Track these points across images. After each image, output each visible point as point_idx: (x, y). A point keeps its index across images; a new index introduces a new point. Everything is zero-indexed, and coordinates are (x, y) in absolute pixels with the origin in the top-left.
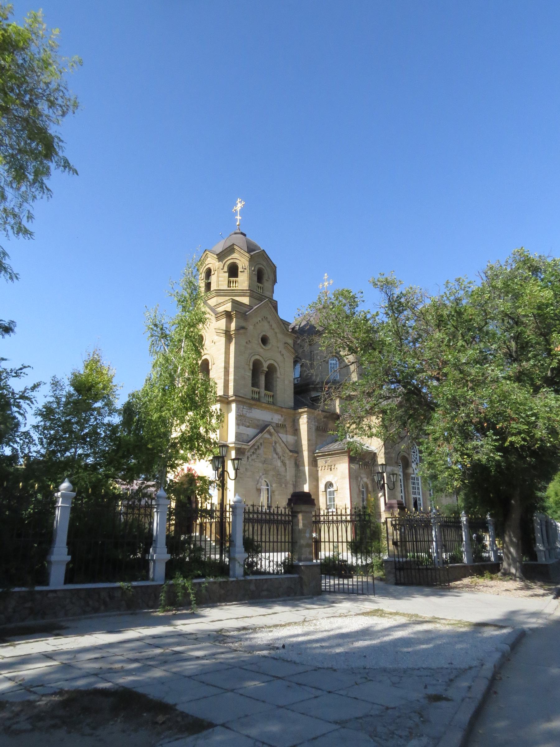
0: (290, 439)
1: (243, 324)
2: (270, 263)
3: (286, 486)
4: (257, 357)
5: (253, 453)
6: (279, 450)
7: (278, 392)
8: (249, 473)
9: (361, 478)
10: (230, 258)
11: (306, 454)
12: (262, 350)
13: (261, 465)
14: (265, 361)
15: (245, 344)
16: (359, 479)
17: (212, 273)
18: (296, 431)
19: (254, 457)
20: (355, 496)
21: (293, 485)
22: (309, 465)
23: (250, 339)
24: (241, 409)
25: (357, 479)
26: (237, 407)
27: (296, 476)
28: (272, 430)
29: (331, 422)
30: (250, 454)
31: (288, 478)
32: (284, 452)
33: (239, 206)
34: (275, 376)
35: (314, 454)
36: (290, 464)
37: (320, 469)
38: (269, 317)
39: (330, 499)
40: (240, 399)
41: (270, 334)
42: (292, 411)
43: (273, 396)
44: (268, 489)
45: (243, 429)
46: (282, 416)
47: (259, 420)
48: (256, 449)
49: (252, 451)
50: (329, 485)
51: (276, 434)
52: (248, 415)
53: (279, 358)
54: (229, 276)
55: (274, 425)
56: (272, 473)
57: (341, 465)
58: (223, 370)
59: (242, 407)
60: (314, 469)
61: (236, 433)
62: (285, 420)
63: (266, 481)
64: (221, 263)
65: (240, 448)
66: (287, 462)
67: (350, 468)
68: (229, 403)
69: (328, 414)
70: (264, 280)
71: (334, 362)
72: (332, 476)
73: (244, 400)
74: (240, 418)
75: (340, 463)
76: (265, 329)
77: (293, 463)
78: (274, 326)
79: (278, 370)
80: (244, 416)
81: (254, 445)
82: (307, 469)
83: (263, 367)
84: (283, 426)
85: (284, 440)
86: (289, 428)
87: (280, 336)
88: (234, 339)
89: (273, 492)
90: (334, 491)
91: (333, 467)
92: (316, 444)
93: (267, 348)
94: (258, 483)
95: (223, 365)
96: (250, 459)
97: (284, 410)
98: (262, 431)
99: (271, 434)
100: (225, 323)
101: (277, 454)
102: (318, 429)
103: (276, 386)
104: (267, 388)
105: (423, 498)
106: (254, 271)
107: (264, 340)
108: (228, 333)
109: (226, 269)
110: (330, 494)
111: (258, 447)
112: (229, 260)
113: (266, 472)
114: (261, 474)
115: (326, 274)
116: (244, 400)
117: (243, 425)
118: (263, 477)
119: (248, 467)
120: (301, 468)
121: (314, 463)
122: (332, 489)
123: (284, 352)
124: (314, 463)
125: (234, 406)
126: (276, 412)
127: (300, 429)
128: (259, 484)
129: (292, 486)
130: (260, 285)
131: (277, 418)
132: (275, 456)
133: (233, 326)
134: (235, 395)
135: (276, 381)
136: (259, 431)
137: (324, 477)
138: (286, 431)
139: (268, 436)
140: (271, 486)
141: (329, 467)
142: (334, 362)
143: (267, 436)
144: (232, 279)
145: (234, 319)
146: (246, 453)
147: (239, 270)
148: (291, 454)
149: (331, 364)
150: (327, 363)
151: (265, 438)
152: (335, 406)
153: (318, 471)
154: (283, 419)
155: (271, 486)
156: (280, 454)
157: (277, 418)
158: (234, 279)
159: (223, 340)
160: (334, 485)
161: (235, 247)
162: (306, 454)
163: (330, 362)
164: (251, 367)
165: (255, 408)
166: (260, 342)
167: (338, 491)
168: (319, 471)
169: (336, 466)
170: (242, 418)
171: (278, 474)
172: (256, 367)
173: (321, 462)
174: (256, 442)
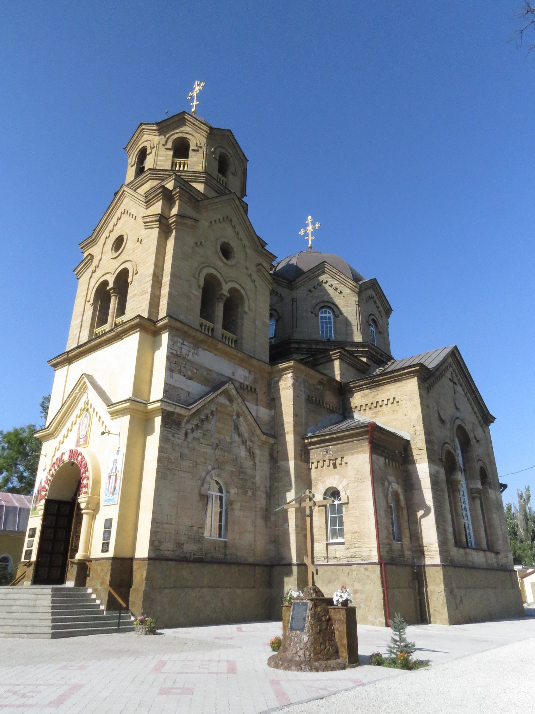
0: (264, 413)
1: (191, 213)
2: (239, 152)
3: (253, 494)
4: (215, 272)
5: (197, 426)
6: (243, 428)
7: (244, 335)
8: (186, 464)
9: (389, 483)
10: (177, 131)
11: (290, 438)
12: (221, 264)
13: (210, 451)
14: (226, 282)
15: (194, 245)
16: (386, 484)
17: (148, 152)
18: (273, 402)
19: (198, 434)
20: (382, 513)
21: (267, 493)
22: (295, 458)
23: (203, 242)
24: (179, 345)
25: (383, 484)
26: (170, 339)
27: (270, 479)
28: (234, 392)
29: (328, 392)
30: (190, 426)
31: (258, 479)
32: (252, 433)
33: (197, 89)
34: (240, 310)
35: (304, 439)
36: (262, 456)
37: (314, 465)
38: (234, 219)
39: (333, 520)
40: (178, 325)
41: (234, 244)
42: (267, 368)
43: (236, 341)
44: (221, 498)
45: (180, 381)
46: (250, 372)
47: (211, 371)
48: (202, 421)
49: (195, 422)
50: (334, 493)
51: (240, 400)
52: (190, 357)
53: (249, 285)
54: (175, 156)
55: (237, 385)
56: (229, 468)
57: (356, 456)
58: (151, 277)
59: (180, 341)
60: (304, 465)
61: (166, 384)
62: (255, 381)
63: (218, 483)
64: (162, 137)
65: (173, 413)
66: (257, 452)
67: (372, 463)
68: (156, 333)
69: (325, 378)
70: (229, 173)
71: (327, 315)
72: (337, 477)
73: (186, 329)
74: (175, 360)
75: (353, 454)
76: (228, 235)
77: (267, 454)
78: (242, 235)
79: (246, 301)
80: (184, 358)
81: (198, 412)
82: (292, 464)
83: (221, 289)
84: (252, 390)
85: (254, 414)
86: (261, 396)
87: (250, 252)
88: (174, 231)
89: (230, 503)
90: (341, 505)
91: (338, 461)
92: (307, 425)
93: (229, 263)
94: (202, 485)
95: (152, 270)
96: (190, 437)
97: (255, 362)
98: (215, 389)
99: (231, 400)
100: (160, 207)
101: (240, 435)
102: (309, 400)
103: (242, 325)
104: (226, 326)
105: (473, 524)
106: (213, 153)
107: (226, 251)
108: (164, 221)
109: (170, 145)
110: (333, 512)
111: (207, 417)
112: (176, 134)
113: (219, 465)
114: (210, 468)
115: (310, 217)
116: (186, 329)
117: (180, 372)
118: (213, 472)
119: (186, 451)
120: (281, 463)
121: (303, 455)
122: (336, 502)
123: (255, 276)
124: (303, 455)
125: (165, 337)
126: (242, 363)
127: (279, 398)
128: (206, 486)
129: (264, 496)
130: (223, 178)
131: (241, 375)
132: (236, 438)
133: (175, 211)
134: (168, 315)
135: (242, 318)
136: (208, 389)
137: (323, 479)
138: (257, 400)
139: (227, 402)
140: (228, 492)
141: (332, 462)
142: (327, 315)
143: (223, 400)
144: (178, 160)
145: (177, 202)
146: (183, 425)
147: (190, 149)
148: (264, 438)
149: (322, 317)
150: (316, 315)
151: (221, 405)
152: (333, 368)
153: (310, 469)
154: (251, 378)
155: (228, 492)
156: (246, 435)
157: (241, 375)
158: (182, 160)
159: (155, 232)
160: (342, 494)
161: (186, 116)
162: (290, 438)
163: (321, 315)
164: (202, 283)
165: (204, 349)
166: (219, 250)
167: (350, 505)
168: (313, 470)
169: (345, 460)
170: (180, 360)
171: (241, 471)
172: (210, 290)
173: (315, 454)
174: (204, 406)
